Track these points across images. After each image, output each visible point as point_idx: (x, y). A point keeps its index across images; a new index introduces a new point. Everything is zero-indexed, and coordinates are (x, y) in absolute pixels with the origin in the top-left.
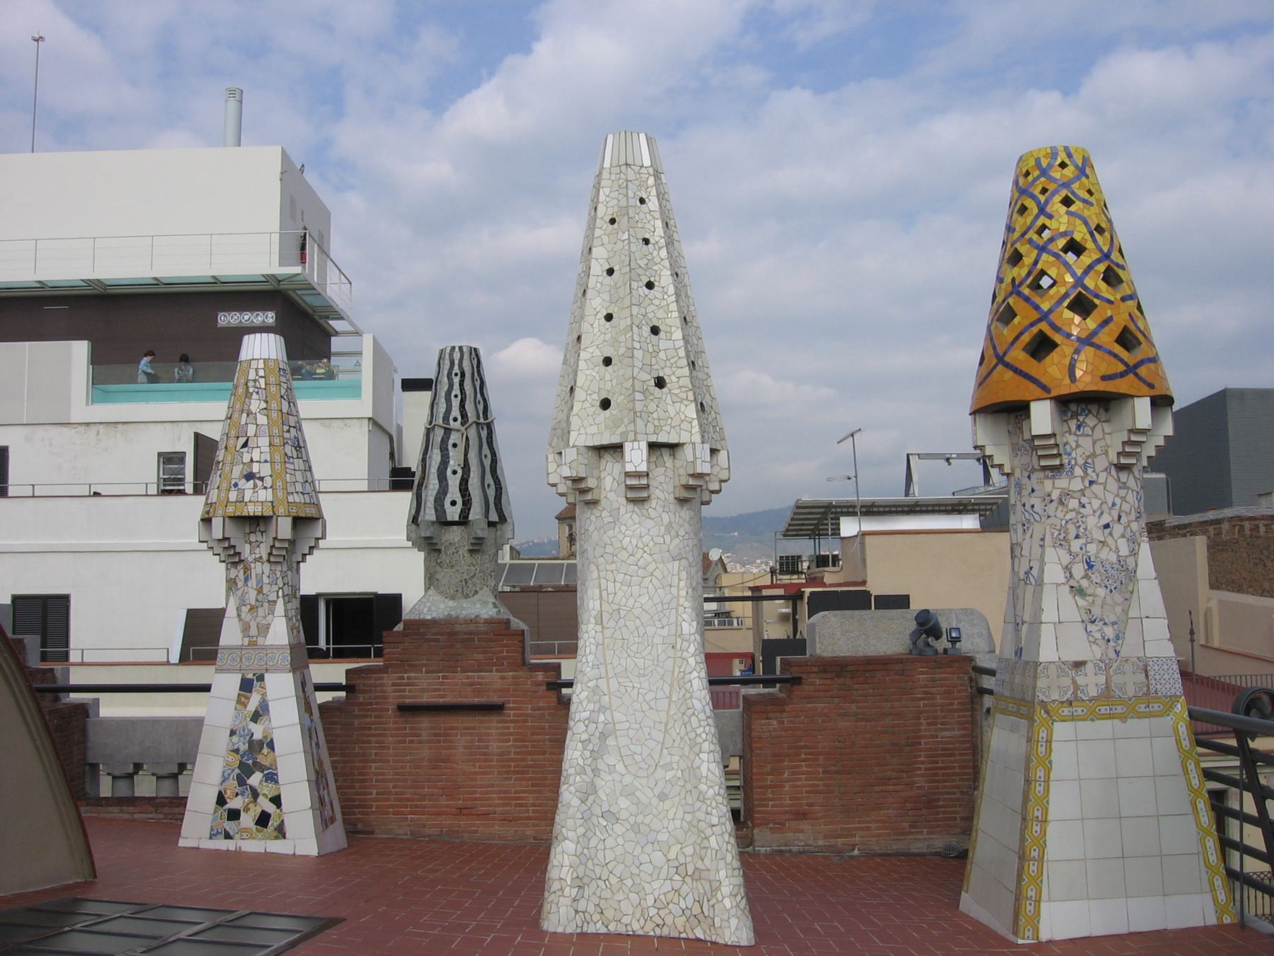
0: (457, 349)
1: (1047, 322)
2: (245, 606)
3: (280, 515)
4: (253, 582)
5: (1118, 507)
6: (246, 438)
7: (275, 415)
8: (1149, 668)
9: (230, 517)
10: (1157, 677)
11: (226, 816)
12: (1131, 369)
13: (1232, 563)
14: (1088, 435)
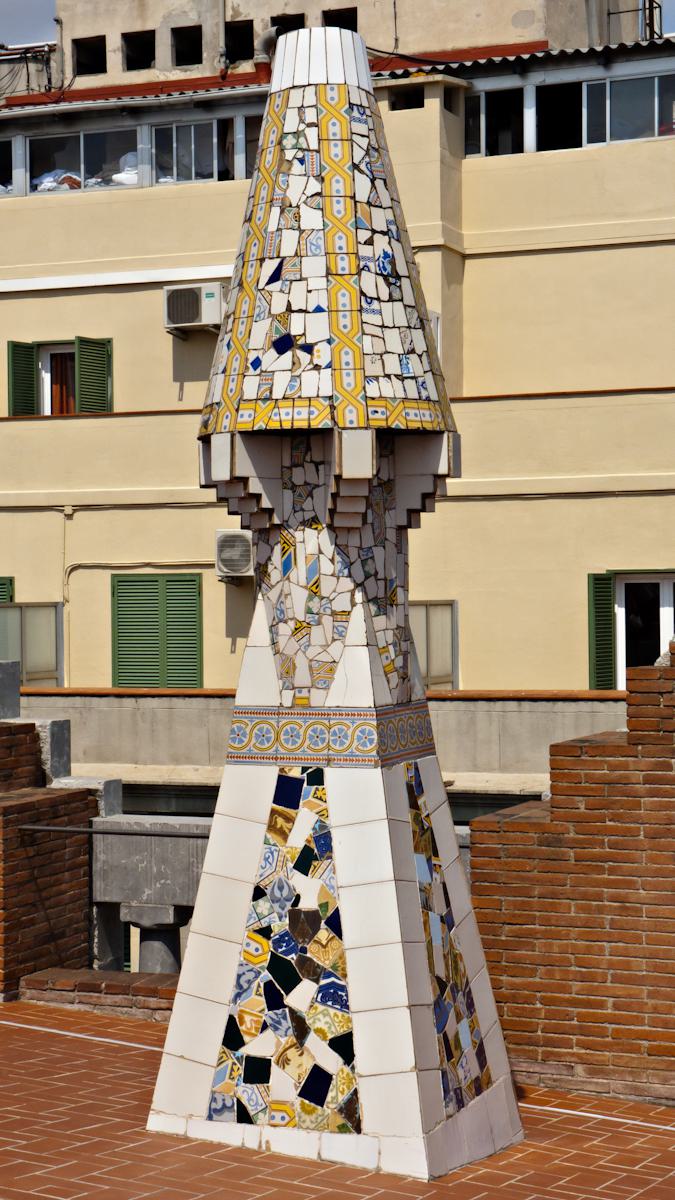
2: (286, 622)
3: (348, 425)
4: (300, 572)
6: (279, 260)
7: (340, 208)
9: (243, 433)
11: (242, 1072)
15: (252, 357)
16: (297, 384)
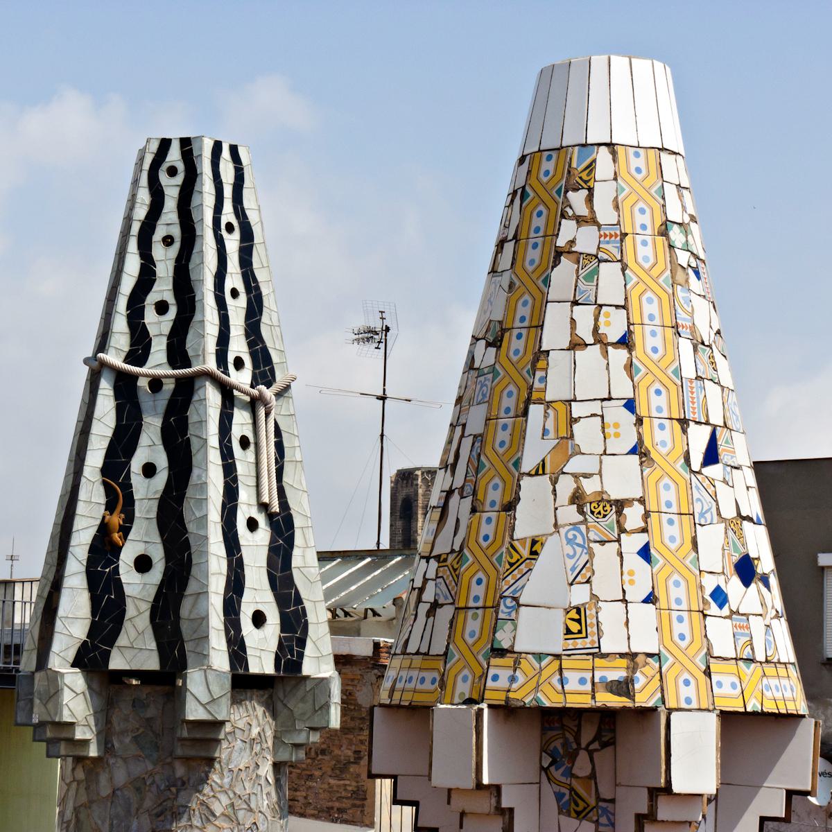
0: (226, 153)
6: (708, 429)
15: (710, 584)
16: (771, 639)
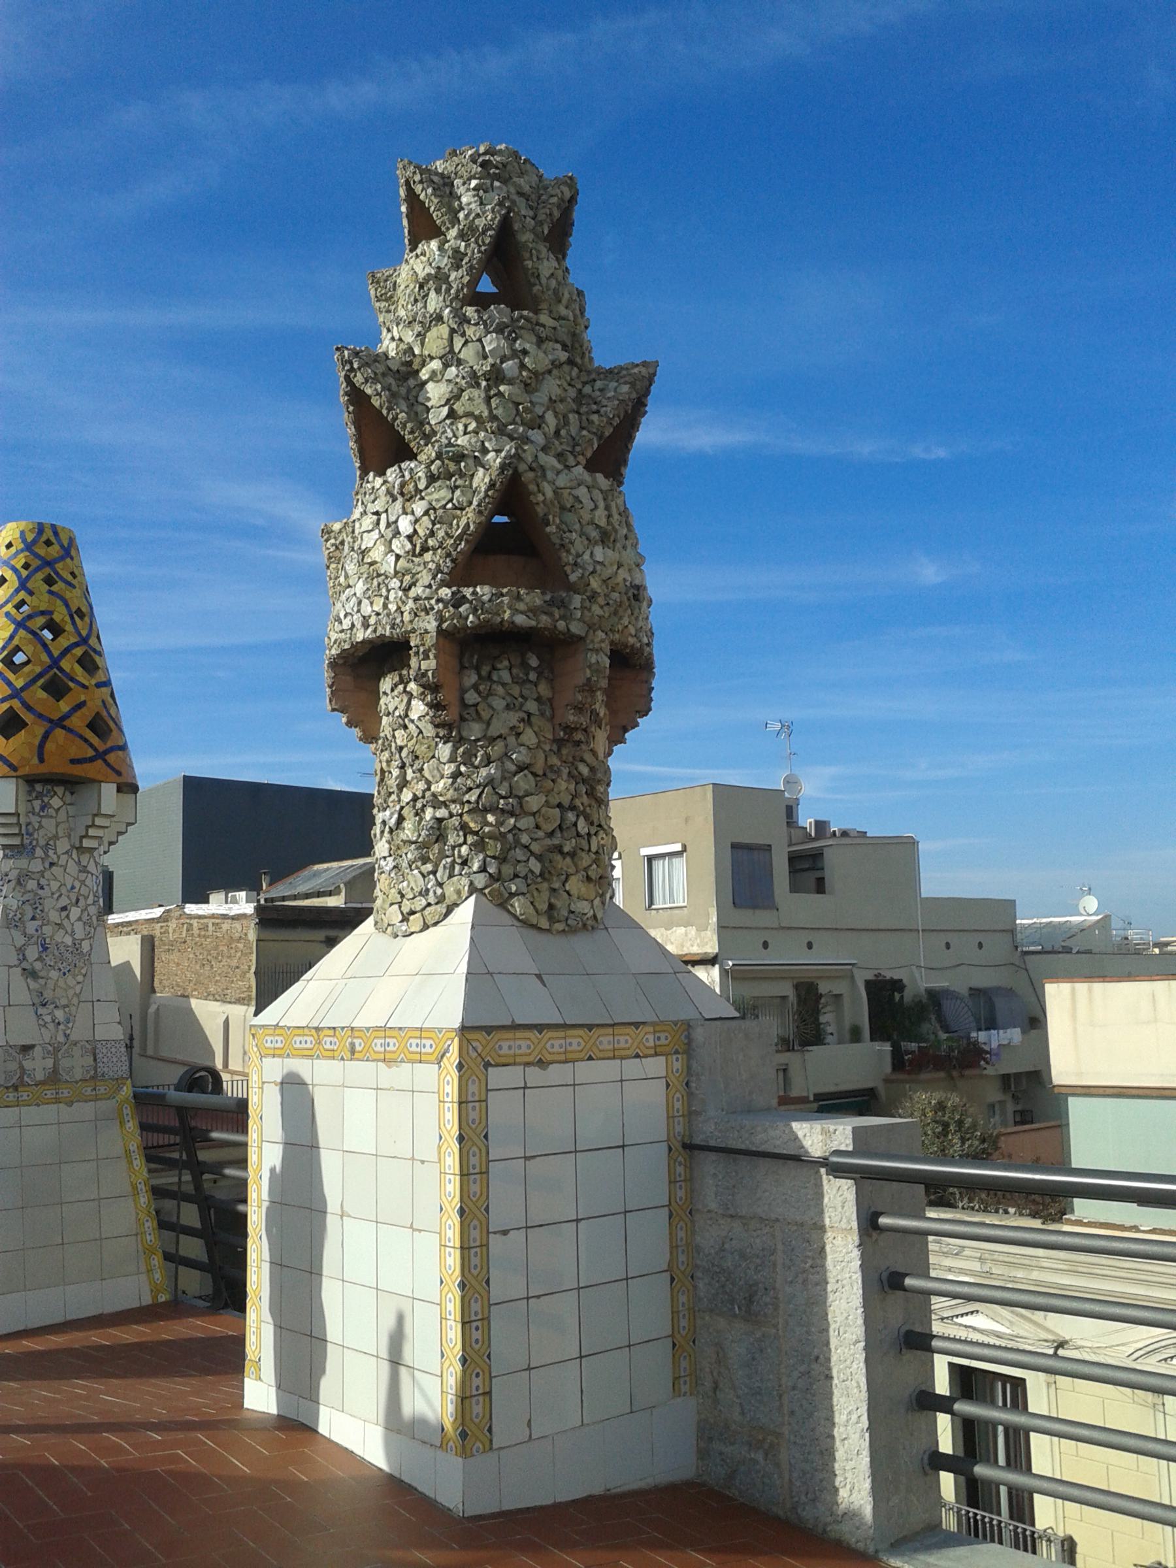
1: (19, 699)
5: (76, 890)
8: (97, 1051)
10: (105, 1060)
12: (101, 755)
13: (178, 964)
14: (52, 817)
